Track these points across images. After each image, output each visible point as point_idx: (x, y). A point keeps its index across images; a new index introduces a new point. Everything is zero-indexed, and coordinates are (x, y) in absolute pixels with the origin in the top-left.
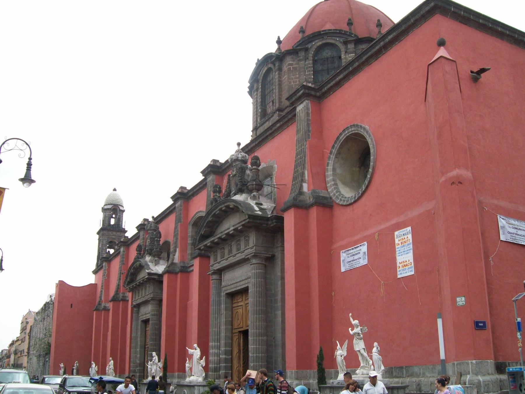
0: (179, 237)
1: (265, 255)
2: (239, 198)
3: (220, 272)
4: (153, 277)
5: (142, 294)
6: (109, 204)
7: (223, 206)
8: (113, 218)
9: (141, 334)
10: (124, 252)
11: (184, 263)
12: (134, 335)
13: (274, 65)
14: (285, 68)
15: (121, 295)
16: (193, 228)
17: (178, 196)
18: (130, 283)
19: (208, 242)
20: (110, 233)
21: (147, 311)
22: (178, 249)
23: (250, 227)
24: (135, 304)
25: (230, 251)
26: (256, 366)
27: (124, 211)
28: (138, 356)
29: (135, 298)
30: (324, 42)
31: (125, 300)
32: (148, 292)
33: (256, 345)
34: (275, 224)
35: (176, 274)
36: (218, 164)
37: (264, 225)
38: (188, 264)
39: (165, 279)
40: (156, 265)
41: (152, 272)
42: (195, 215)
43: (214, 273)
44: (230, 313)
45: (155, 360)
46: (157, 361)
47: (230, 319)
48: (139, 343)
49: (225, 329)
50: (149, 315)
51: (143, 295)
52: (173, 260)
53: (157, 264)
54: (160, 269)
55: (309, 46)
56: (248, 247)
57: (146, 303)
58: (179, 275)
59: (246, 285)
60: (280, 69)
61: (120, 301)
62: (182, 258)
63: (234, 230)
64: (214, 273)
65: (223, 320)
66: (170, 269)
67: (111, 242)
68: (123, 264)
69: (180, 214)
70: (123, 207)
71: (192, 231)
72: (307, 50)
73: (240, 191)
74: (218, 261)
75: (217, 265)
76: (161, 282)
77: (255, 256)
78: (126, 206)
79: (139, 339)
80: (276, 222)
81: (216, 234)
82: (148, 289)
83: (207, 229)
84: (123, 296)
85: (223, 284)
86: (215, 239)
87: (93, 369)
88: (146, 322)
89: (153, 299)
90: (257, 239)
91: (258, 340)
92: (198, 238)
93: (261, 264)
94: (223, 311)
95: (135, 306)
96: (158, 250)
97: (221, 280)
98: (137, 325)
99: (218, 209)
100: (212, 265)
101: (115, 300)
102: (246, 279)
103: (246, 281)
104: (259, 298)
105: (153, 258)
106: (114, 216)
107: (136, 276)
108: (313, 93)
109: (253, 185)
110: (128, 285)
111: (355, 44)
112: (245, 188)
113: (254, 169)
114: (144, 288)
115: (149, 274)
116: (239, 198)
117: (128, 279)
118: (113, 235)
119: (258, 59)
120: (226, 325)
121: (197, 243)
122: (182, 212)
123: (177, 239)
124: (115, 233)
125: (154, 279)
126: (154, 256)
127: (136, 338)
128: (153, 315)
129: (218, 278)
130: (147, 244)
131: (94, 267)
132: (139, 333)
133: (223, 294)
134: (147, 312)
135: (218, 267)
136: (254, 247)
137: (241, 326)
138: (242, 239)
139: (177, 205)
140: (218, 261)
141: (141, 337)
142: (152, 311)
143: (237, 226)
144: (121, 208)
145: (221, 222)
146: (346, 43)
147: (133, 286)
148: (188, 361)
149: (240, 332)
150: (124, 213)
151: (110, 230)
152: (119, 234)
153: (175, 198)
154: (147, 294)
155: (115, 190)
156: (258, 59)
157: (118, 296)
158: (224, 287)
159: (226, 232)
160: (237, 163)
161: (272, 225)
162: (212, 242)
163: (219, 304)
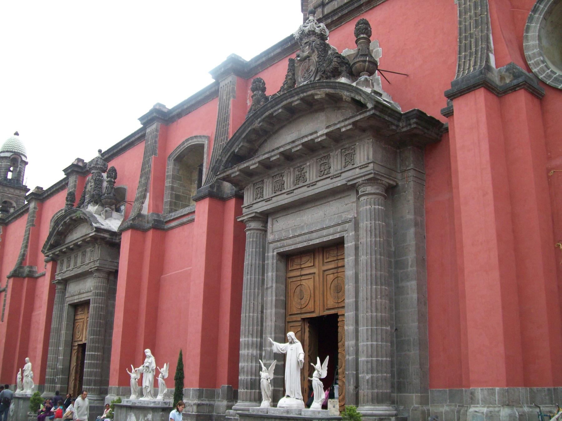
0: (152, 176)
1: (387, 181)
3: (264, 217)
4: (102, 235)
5: (76, 263)
6: (7, 151)
7: (296, 98)
8: (10, 171)
9: (67, 324)
10: (35, 208)
11: (158, 215)
12: (54, 325)
15: (26, 270)
16: (175, 165)
17: (155, 114)
18: (53, 247)
20: (6, 189)
21: (86, 289)
22: (148, 194)
23: (364, 130)
24: (60, 278)
25: (300, 178)
26: (377, 380)
27: (26, 163)
28: (61, 357)
29: (61, 270)
31: (33, 277)
32: (92, 258)
33: (377, 341)
34: (415, 126)
35: (145, 231)
37: (394, 127)
38: (165, 217)
40: (106, 218)
41: (102, 227)
42: (183, 143)
43: (254, 219)
44: (283, 287)
45: (150, 363)
46: (154, 365)
47: (282, 298)
48: (63, 338)
49: (276, 314)
50: (90, 294)
51: (79, 263)
52: (141, 209)
53: (108, 216)
54: (113, 224)
56: (350, 167)
58: (150, 234)
59: (338, 236)
61: (25, 278)
62: (156, 209)
63: (327, 134)
64: (254, 219)
65: (271, 298)
66: (136, 222)
67: (5, 202)
68: (33, 225)
69: (155, 142)
70: (26, 157)
71: (174, 169)
74: (265, 198)
75: (263, 203)
77: (372, 181)
78: (30, 157)
79: (63, 332)
80: (416, 123)
81: (259, 153)
82: (88, 255)
83: (246, 144)
84: (30, 271)
85: (270, 237)
86: (252, 164)
89: (98, 270)
90: (375, 152)
91: (379, 331)
92: (224, 160)
93: (381, 195)
95: (59, 282)
96: (111, 195)
97: (266, 231)
98: (61, 310)
99: (280, 106)
100: (249, 207)
101: (16, 275)
102: (339, 224)
103: (339, 228)
104: (380, 255)
105: (101, 208)
106: (12, 169)
107: (65, 236)
109: (365, 61)
110: (49, 250)
112: (344, 68)
113: (363, 38)
114: (65, 260)
115: (98, 230)
117: (52, 241)
120: (276, 307)
121: (222, 167)
122: (157, 139)
123: (148, 178)
124: (12, 190)
125: (103, 239)
126: (103, 205)
127: (59, 330)
128: (97, 294)
129: (260, 227)
130: (89, 188)
132: (64, 323)
133: (271, 254)
134: (82, 291)
135: (265, 208)
136: (371, 166)
137: (310, 307)
139: (148, 130)
141: (67, 329)
142: (96, 288)
143: (338, 126)
144: (24, 159)
145: (276, 132)
147: (61, 251)
148: (264, 368)
149: (304, 320)
150: (27, 166)
151: (6, 186)
152: (17, 192)
153: (147, 121)
154: (87, 262)
155: (17, 134)
157: (21, 270)
158: (271, 243)
159: (282, 150)
160: (313, 38)
161: (405, 129)
163: (263, 270)
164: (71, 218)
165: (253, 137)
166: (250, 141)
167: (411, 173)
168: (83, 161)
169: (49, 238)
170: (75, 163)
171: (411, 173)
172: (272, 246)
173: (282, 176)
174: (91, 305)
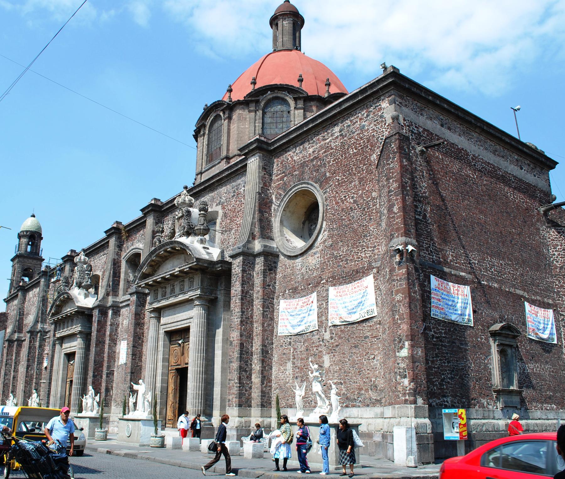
2: (184, 240)
13: (224, 113)
14: (235, 116)
18: (53, 315)
19: (150, 281)
23: (196, 270)
25: (173, 291)
30: (274, 95)
36: (159, 204)
39: (96, 313)
44: (168, 350)
47: (167, 356)
55: (261, 98)
56: (192, 288)
57: (71, 337)
60: (230, 118)
65: (160, 357)
67: (26, 270)
72: (257, 102)
73: (188, 234)
74: (159, 299)
76: (91, 316)
87: (33, 400)
88: (70, 356)
89: (80, 332)
94: (161, 348)
98: (59, 358)
103: (188, 321)
108: (265, 146)
111: (304, 101)
116: (184, 240)
117: (53, 311)
118: (29, 263)
119: (206, 105)
129: (157, 316)
131: (6, 295)
133: (162, 332)
138: (186, 280)
140: (159, 299)
141: (63, 370)
142: (79, 344)
146: (295, 99)
147: (58, 318)
149: (176, 369)
152: (35, 261)
156: (206, 105)
162: (155, 281)
164: (64, 297)
165: (153, 263)
166: (151, 266)
167: (223, 292)
168: (75, 251)
169: (51, 309)
170: (69, 254)
171: (223, 292)
172: (162, 327)
173: (166, 288)
174: (76, 355)
